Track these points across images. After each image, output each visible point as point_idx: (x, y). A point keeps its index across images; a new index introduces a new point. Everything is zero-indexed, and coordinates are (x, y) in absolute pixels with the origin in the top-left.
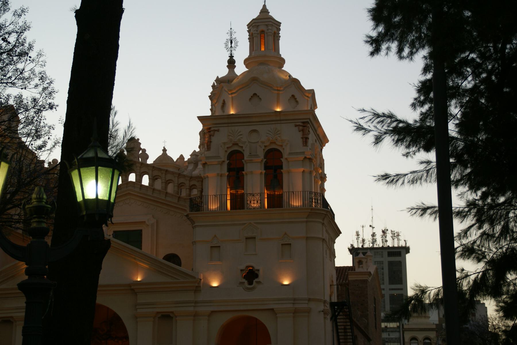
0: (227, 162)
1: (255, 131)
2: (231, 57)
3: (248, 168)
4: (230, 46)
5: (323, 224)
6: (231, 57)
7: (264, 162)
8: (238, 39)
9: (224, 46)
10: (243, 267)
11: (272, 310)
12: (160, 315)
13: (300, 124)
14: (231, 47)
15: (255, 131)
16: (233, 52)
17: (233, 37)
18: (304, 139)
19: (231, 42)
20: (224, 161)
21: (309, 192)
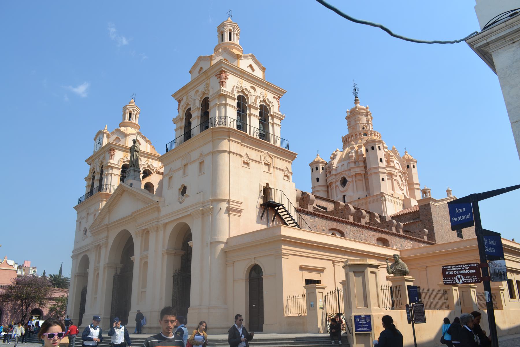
0: (185, 118)
1: (197, 91)
2: (356, 97)
3: (193, 116)
4: (355, 92)
5: (229, 140)
6: (356, 97)
7: (201, 109)
8: (358, 87)
9: (352, 93)
10: (180, 187)
11: (190, 215)
12: (145, 232)
13: (218, 73)
14: (356, 93)
15: (197, 91)
16: (357, 95)
17: (356, 87)
18: (221, 83)
19: (356, 90)
20: (183, 118)
21: (214, 118)
